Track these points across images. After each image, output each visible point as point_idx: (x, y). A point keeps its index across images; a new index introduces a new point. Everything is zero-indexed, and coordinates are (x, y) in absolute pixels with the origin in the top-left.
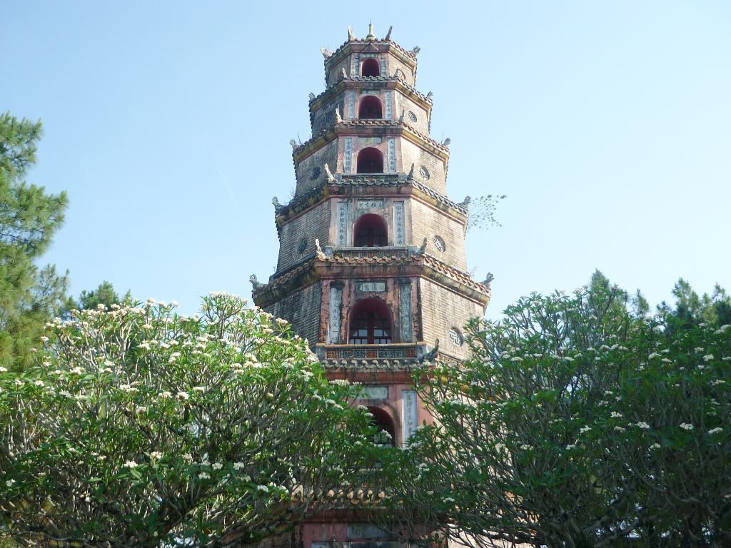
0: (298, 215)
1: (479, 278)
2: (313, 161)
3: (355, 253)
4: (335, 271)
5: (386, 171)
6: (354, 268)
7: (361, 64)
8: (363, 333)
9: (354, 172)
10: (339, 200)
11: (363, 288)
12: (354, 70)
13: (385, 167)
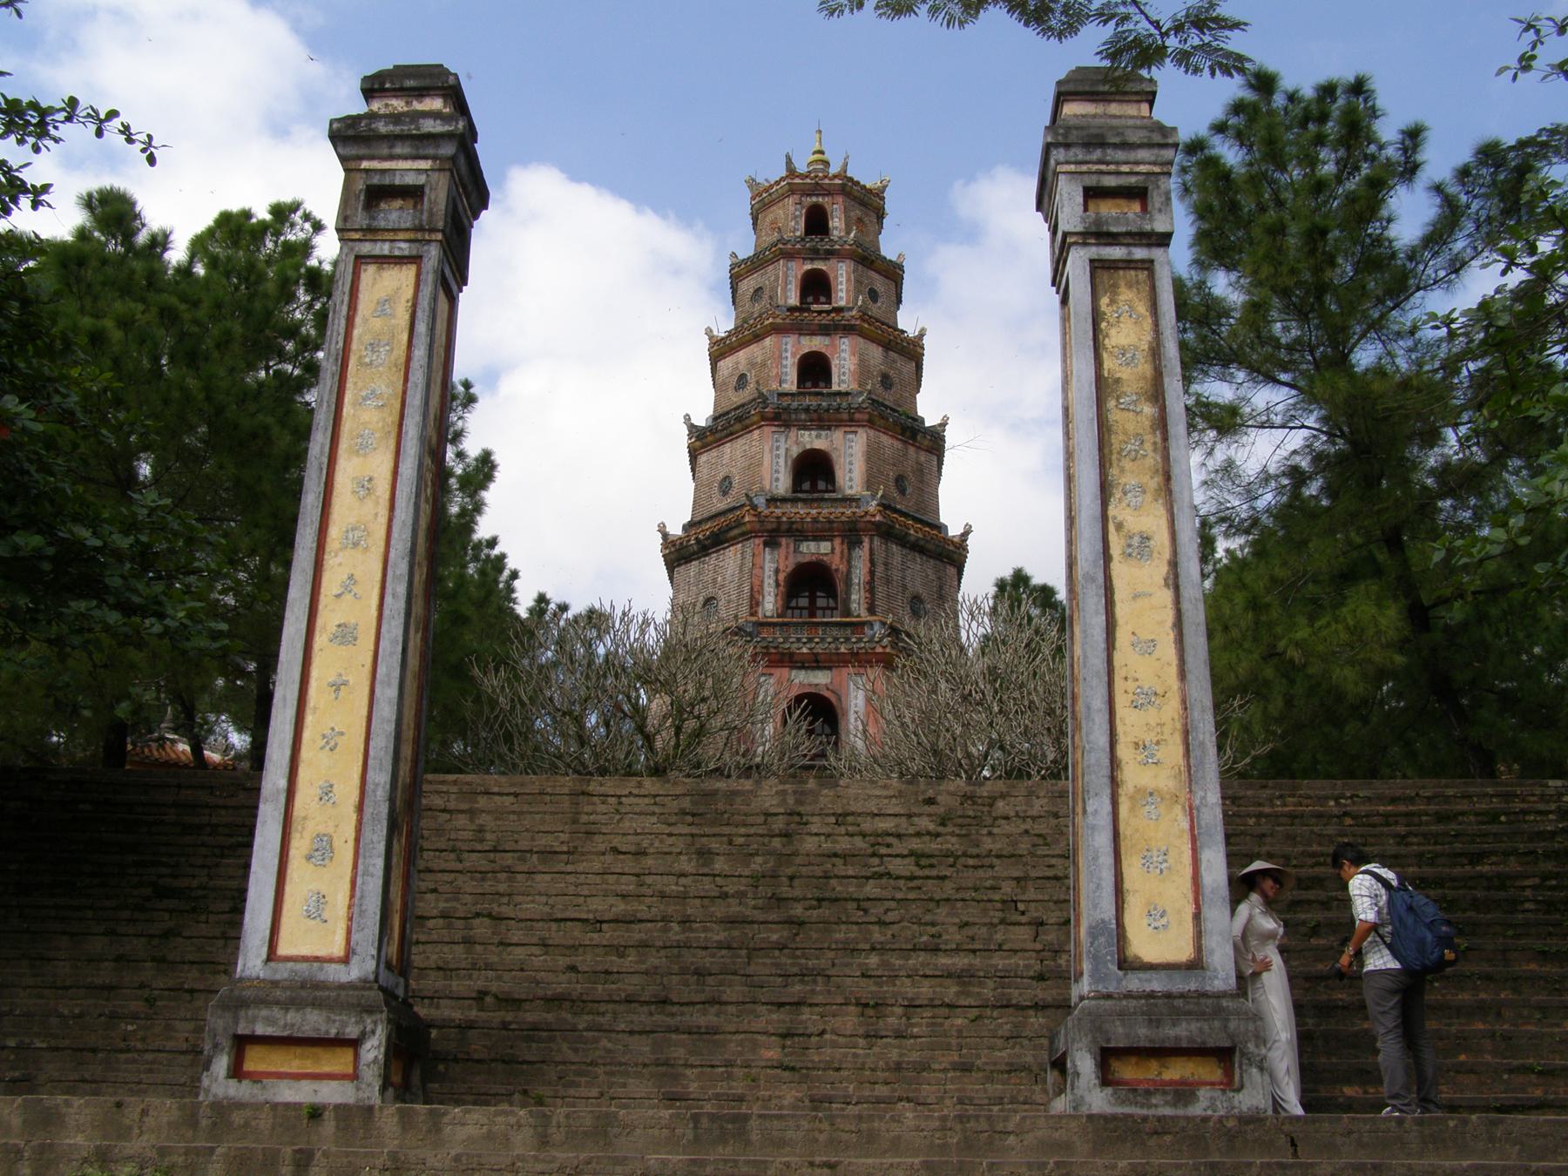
0: (719, 442)
1: (954, 531)
3: (794, 501)
4: (770, 527)
5: (835, 388)
8: (804, 602)
9: (794, 388)
12: (791, 220)
13: (835, 379)
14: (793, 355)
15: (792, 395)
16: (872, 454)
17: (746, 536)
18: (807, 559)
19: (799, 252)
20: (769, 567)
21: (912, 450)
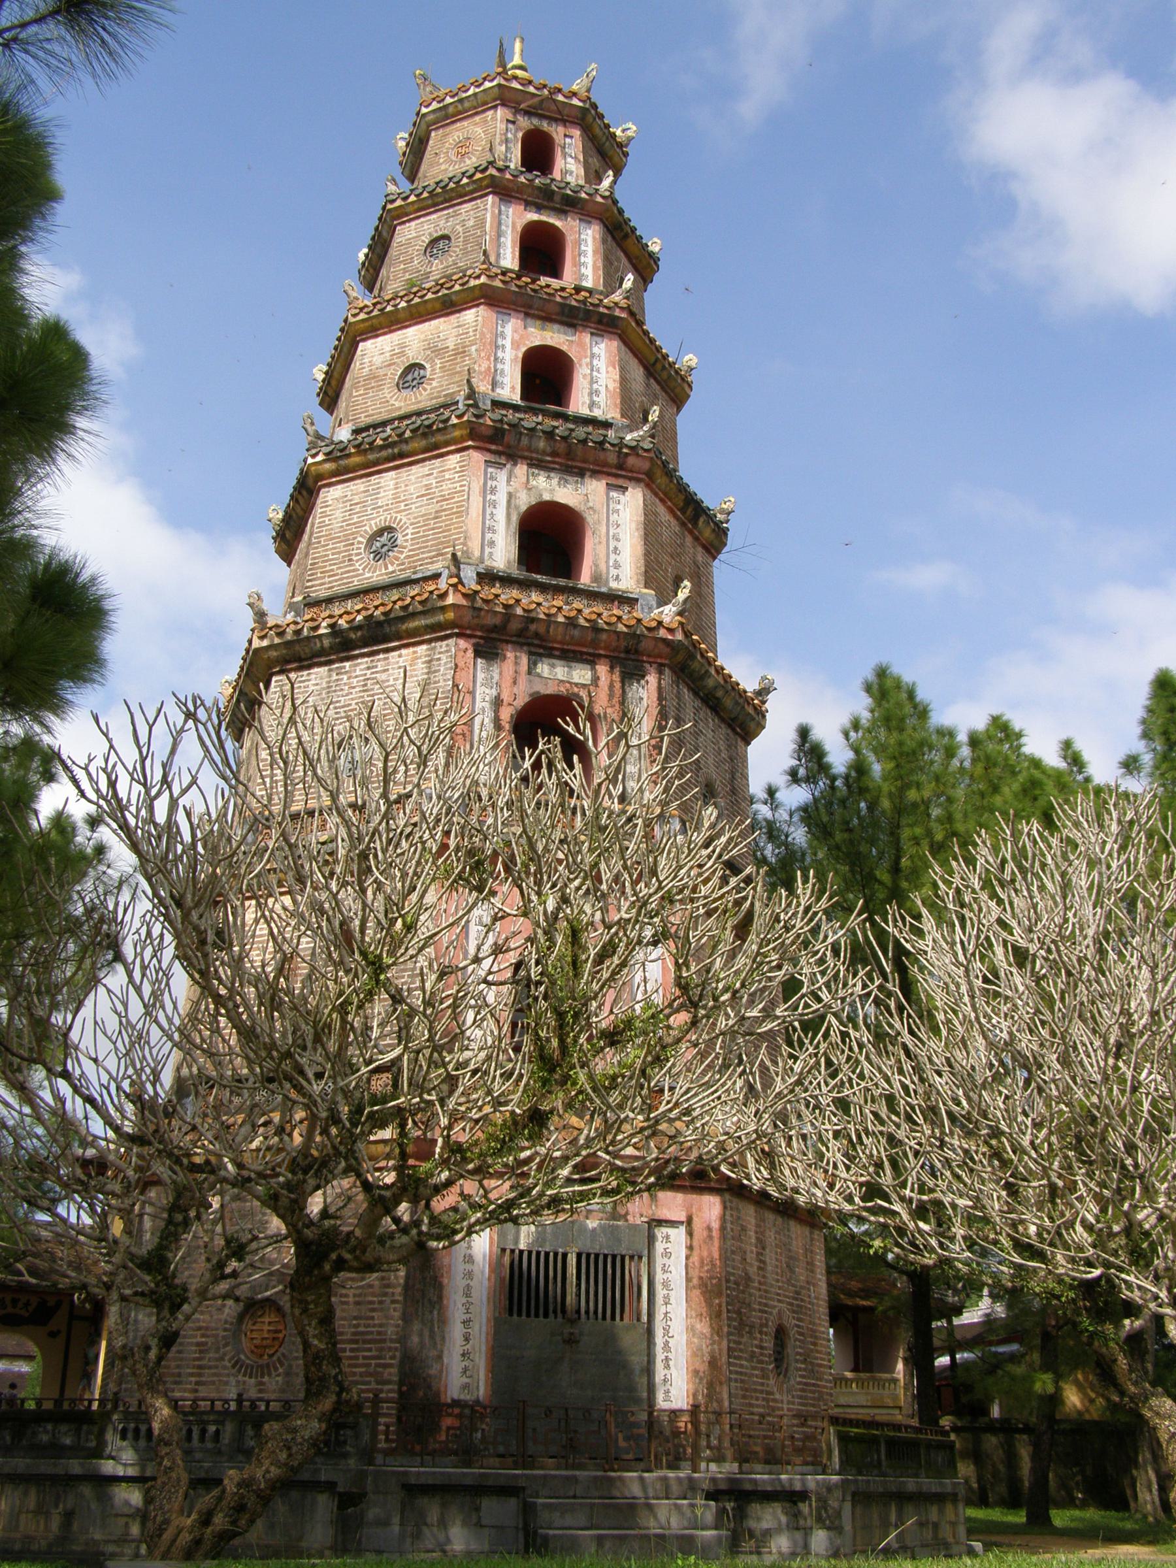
1: (749, 685)
2: (402, 346)
3: (525, 585)
4: (490, 621)
6: (533, 620)
7: (520, 135)
9: (516, 397)
10: (489, 457)
11: (543, 668)
14: (515, 345)
15: (515, 408)
16: (650, 530)
17: (437, 632)
18: (550, 690)
19: (521, 188)
20: (483, 696)
21: (689, 539)
